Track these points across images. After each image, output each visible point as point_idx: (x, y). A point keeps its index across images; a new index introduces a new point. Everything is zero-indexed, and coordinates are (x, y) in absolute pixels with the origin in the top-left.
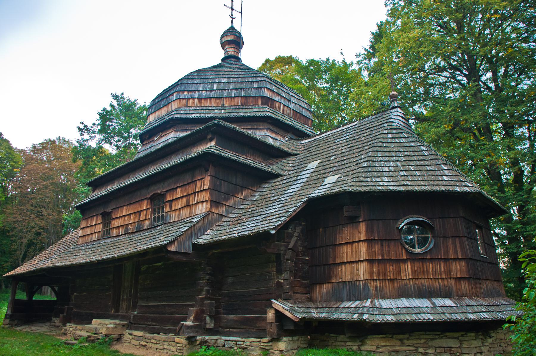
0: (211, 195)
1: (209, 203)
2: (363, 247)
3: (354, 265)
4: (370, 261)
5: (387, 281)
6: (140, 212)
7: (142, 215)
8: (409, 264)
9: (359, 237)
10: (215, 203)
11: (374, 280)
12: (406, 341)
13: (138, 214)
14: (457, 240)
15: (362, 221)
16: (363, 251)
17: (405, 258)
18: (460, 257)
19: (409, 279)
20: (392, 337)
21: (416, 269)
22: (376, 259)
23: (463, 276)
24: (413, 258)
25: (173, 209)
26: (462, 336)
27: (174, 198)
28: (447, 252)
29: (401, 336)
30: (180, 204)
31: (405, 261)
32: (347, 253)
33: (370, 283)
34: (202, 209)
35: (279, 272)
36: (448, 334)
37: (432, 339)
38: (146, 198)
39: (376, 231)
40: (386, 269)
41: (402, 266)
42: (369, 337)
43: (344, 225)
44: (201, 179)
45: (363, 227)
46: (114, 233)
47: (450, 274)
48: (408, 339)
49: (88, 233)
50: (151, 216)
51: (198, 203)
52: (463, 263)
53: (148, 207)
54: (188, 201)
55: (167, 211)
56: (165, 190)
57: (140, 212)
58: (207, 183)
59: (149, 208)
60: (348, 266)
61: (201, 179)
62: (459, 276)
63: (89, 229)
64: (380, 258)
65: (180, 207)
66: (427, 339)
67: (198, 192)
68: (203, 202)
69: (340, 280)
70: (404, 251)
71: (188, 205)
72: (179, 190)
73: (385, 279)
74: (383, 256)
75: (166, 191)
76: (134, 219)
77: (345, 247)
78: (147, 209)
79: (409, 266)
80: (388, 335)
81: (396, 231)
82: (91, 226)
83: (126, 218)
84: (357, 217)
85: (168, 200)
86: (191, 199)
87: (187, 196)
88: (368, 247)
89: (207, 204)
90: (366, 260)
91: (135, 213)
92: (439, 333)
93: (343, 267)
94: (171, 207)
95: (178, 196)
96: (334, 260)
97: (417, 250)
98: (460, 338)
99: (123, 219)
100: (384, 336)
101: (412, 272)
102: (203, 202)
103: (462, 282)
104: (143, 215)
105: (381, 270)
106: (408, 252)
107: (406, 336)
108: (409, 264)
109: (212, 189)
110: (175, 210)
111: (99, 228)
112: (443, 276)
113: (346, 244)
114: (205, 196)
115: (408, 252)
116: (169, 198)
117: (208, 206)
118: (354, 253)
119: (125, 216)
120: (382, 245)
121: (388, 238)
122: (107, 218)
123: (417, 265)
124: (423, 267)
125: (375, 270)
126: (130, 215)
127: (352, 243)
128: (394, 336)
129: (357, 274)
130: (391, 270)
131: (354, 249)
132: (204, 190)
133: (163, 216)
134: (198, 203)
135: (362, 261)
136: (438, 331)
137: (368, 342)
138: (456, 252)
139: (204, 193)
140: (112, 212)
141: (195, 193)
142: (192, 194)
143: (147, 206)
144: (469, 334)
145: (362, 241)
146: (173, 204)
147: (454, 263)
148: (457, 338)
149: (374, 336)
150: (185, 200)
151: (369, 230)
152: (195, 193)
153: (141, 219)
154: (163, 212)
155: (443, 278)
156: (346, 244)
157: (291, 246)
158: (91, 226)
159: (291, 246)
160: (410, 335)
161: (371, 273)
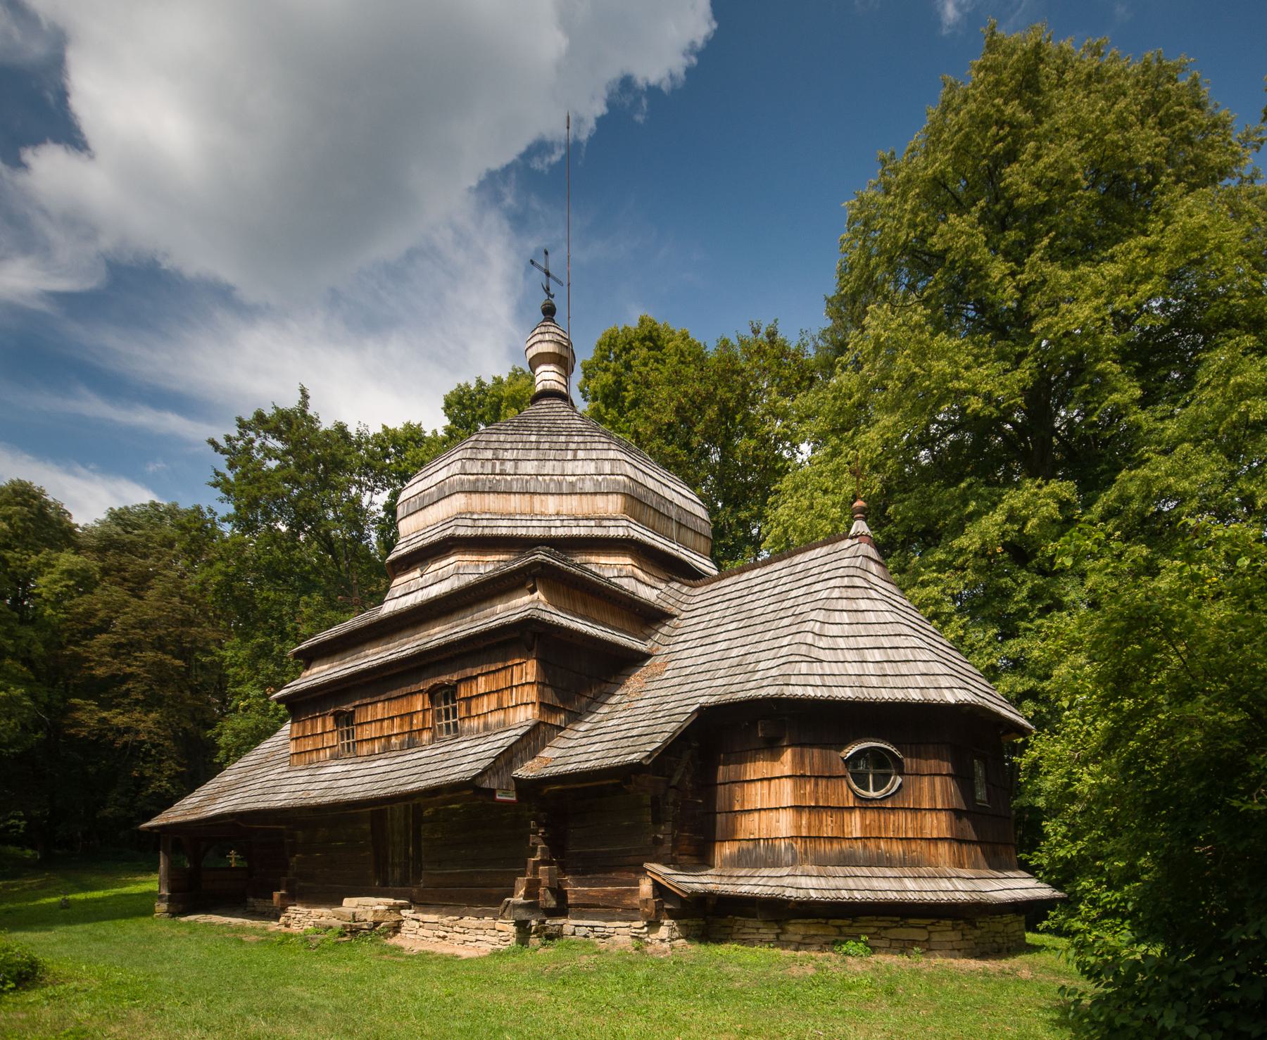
0: (541, 693)
2: (788, 785)
3: (773, 814)
4: (798, 808)
5: (822, 840)
6: (411, 714)
7: (415, 721)
8: (858, 812)
9: (782, 771)
10: (545, 707)
11: (801, 837)
12: (846, 930)
13: (407, 719)
14: (938, 780)
15: (788, 746)
16: (786, 793)
17: (851, 805)
18: (939, 807)
19: (856, 839)
20: (826, 923)
21: (868, 822)
22: (805, 807)
23: (941, 836)
24: (865, 805)
26: (932, 924)
27: (475, 694)
28: (918, 799)
29: (839, 922)
30: (486, 704)
31: (851, 809)
32: (762, 795)
33: (796, 843)
34: (525, 716)
35: (657, 821)
36: (911, 921)
37: (886, 928)
38: (421, 691)
39: (807, 761)
40: (821, 822)
41: (846, 815)
42: (793, 921)
43: (758, 750)
44: (520, 664)
45: (788, 755)
47: (922, 833)
48: (850, 926)
50: (433, 724)
51: (517, 705)
52: (943, 817)
53: (426, 707)
54: (500, 701)
55: (462, 716)
56: (455, 679)
57: (411, 714)
59: (428, 709)
60: (762, 812)
61: (520, 664)
62: (935, 836)
64: (813, 804)
65: (485, 711)
66: (879, 928)
67: (516, 686)
68: (527, 704)
69: (752, 837)
70: (851, 794)
71: (500, 708)
72: (482, 680)
73: (819, 837)
74: (817, 801)
75: (459, 681)
76: (401, 726)
77: (759, 784)
78: (424, 711)
79: (858, 819)
80: (820, 920)
81: (841, 762)
82: (312, 735)
83: (386, 723)
84: (781, 739)
85: (462, 696)
86: (505, 697)
87: (497, 691)
88: (795, 786)
89: (533, 709)
90: (791, 807)
91: (401, 716)
92: (898, 919)
93: (756, 815)
94: (469, 710)
95: (481, 691)
96: (743, 805)
97: (872, 794)
98: (930, 928)
100: (816, 920)
101: (861, 828)
102: (527, 704)
103: (940, 845)
104: (417, 721)
105: (813, 823)
106: (857, 797)
107: (848, 922)
108: (858, 812)
110: (478, 715)
112: (910, 835)
113: (761, 780)
114: (531, 694)
115: (857, 797)
116: (463, 692)
117: (536, 712)
118: (773, 795)
119: (382, 720)
120: (816, 785)
121: (827, 774)
122: (345, 721)
123: (870, 816)
124: (879, 821)
125: (804, 822)
126: (392, 718)
127: (770, 779)
128: (831, 921)
129: (778, 829)
130: (829, 822)
131: (772, 788)
132: (527, 683)
133: (455, 724)
134: (517, 705)
135: (785, 808)
136: (897, 916)
137: (790, 928)
138: (933, 798)
139: (527, 688)
140: (354, 712)
141: (511, 687)
142: (506, 689)
143: (423, 705)
144: (942, 922)
145: (786, 777)
146: (474, 703)
147: (928, 815)
148: (924, 928)
149: (800, 921)
150: (494, 697)
151: (799, 761)
152: (511, 687)
153: (415, 728)
154: (455, 717)
155: (910, 839)
156: (761, 780)
157: (674, 782)
158: (312, 735)
159: (674, 782)
160: (854, 922)
161: (798, 827)
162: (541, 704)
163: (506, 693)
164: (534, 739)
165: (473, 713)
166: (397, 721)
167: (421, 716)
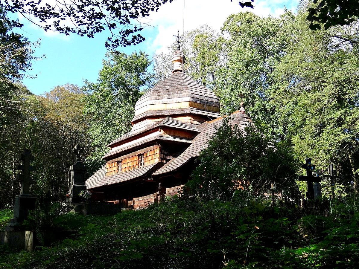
0: (160, 155)
1: (159, 159)
7: (135, 163)
10: (161, 159)
25: (147, 161)
30: (150, 158)
34: (157, 161)
46: (123, 170)
49: (111, 171)
58: (158, 150)
63: (111, 169)
72: (149, 152)
83: (128, 164)
91: (132, 162)
99: (127, 164)
109: (161, 153)
111: (116, 168)
116: (145, 156)
126: (130, 162)
150: (151, 157)
162: (160, 158)
163: (153, 155)
164: (158, 166)
165: (147, 161)
166: (131, 163)
167: (136, 161)
